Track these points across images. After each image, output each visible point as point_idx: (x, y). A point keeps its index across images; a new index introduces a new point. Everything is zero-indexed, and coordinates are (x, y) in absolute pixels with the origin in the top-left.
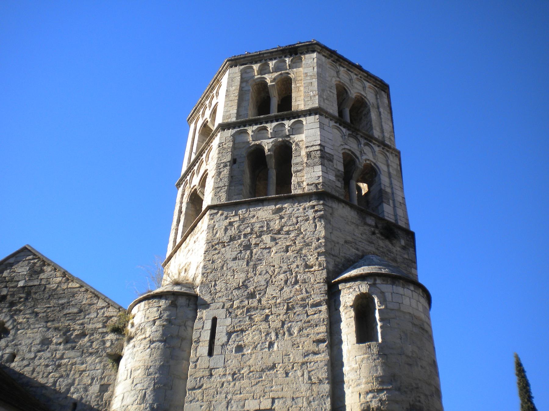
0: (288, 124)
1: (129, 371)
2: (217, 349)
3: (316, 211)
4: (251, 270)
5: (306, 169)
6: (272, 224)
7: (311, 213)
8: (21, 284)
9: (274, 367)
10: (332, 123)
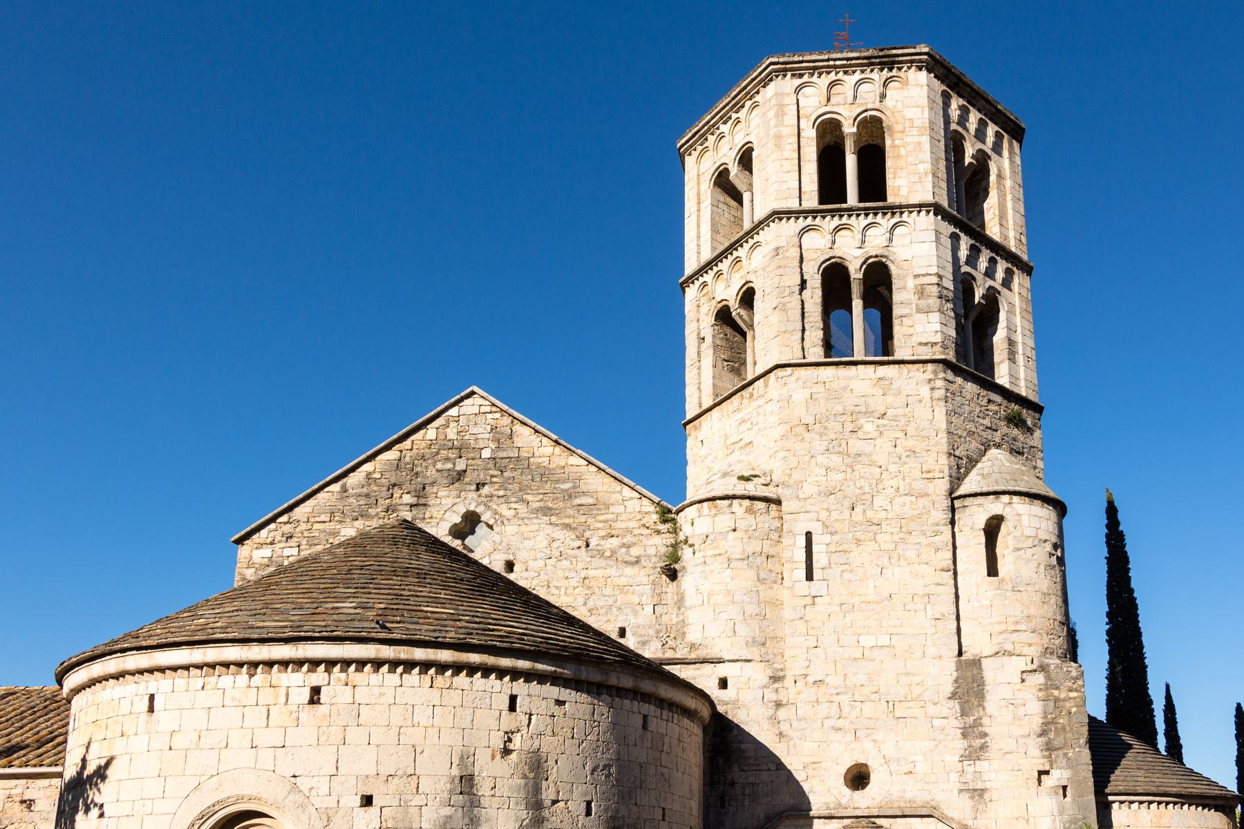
0: (885, 222)
1: (706, 595)
2: (817, 574)
3: (932, 389)
4: (849, 470)
6: (870, 401)
7: (925, 391)
8: (486, 454)
10: (952, 229)
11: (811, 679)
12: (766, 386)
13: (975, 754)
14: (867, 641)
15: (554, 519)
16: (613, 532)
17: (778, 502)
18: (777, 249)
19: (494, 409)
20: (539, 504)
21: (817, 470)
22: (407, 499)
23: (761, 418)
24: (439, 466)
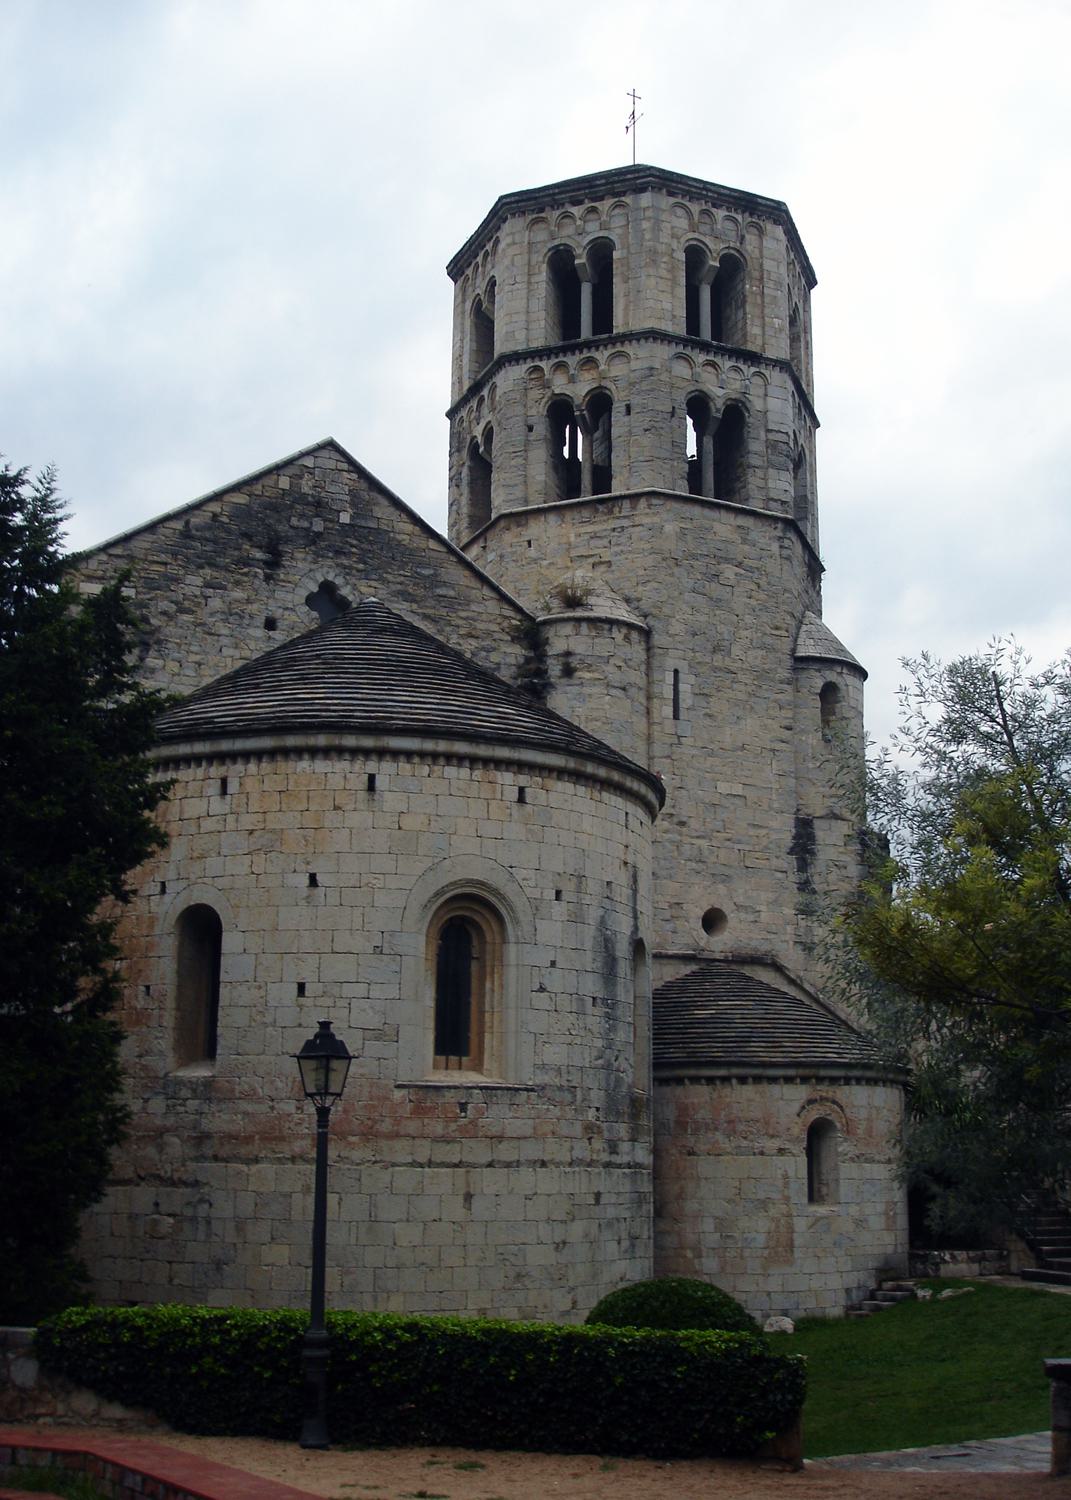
2: (683, 714)
5: (770, 470)
7: (775, 547)
8: (345, 518)
9: (743, 748)
11: (675, 820)
12: (634, 508)
13: (806, 911)
14: (723, 788)
15: (415, 606)
16: (474, 633)
17: (646, 634)
18: (652, 369)
19: (351, 468)
20: (399, 587)
21: (684, 607)
22: (259, 555)
23: (623, 540)
24: (294, 521)
